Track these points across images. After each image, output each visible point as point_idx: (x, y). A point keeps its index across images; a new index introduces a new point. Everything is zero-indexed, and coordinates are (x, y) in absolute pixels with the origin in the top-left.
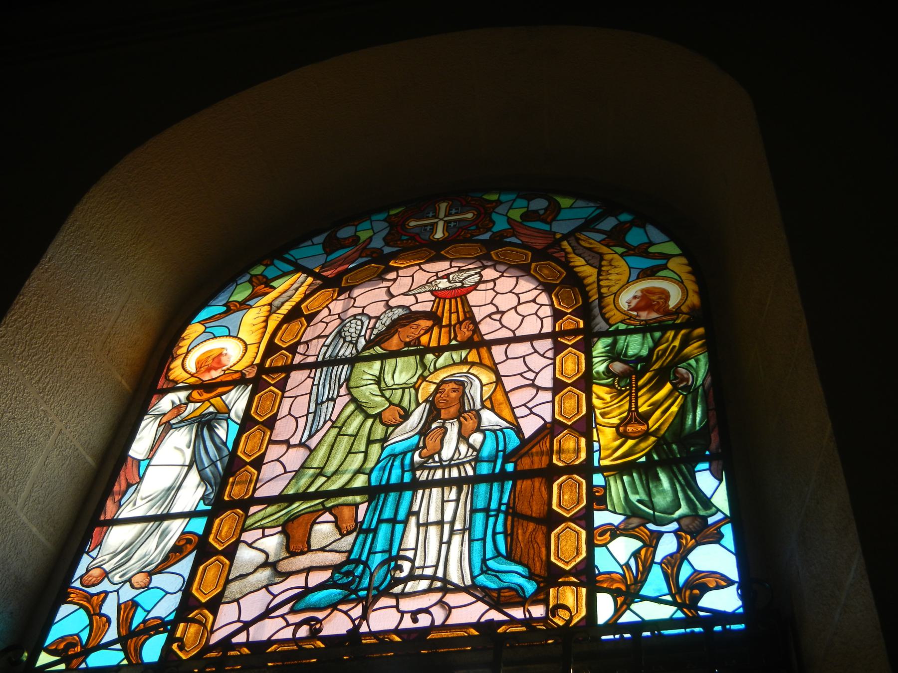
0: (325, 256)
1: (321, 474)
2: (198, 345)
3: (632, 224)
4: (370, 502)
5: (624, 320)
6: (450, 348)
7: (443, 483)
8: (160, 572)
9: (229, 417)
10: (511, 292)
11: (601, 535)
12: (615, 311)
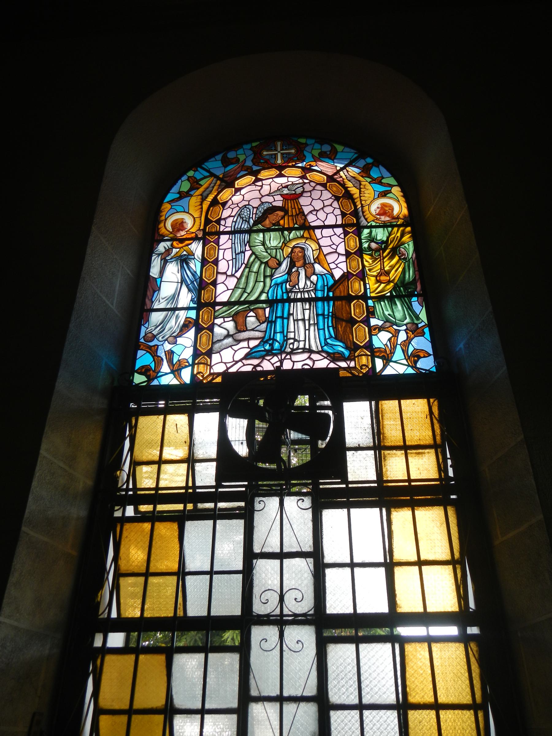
0: (223, 168)
1: (244, 292)
3: (373, 165)
4: (270, 307)
5: (374, 220)
6: (296, 229)
7: (303, 300)
9: (195, 258)
10: (319, 199)
11: (374, 330)
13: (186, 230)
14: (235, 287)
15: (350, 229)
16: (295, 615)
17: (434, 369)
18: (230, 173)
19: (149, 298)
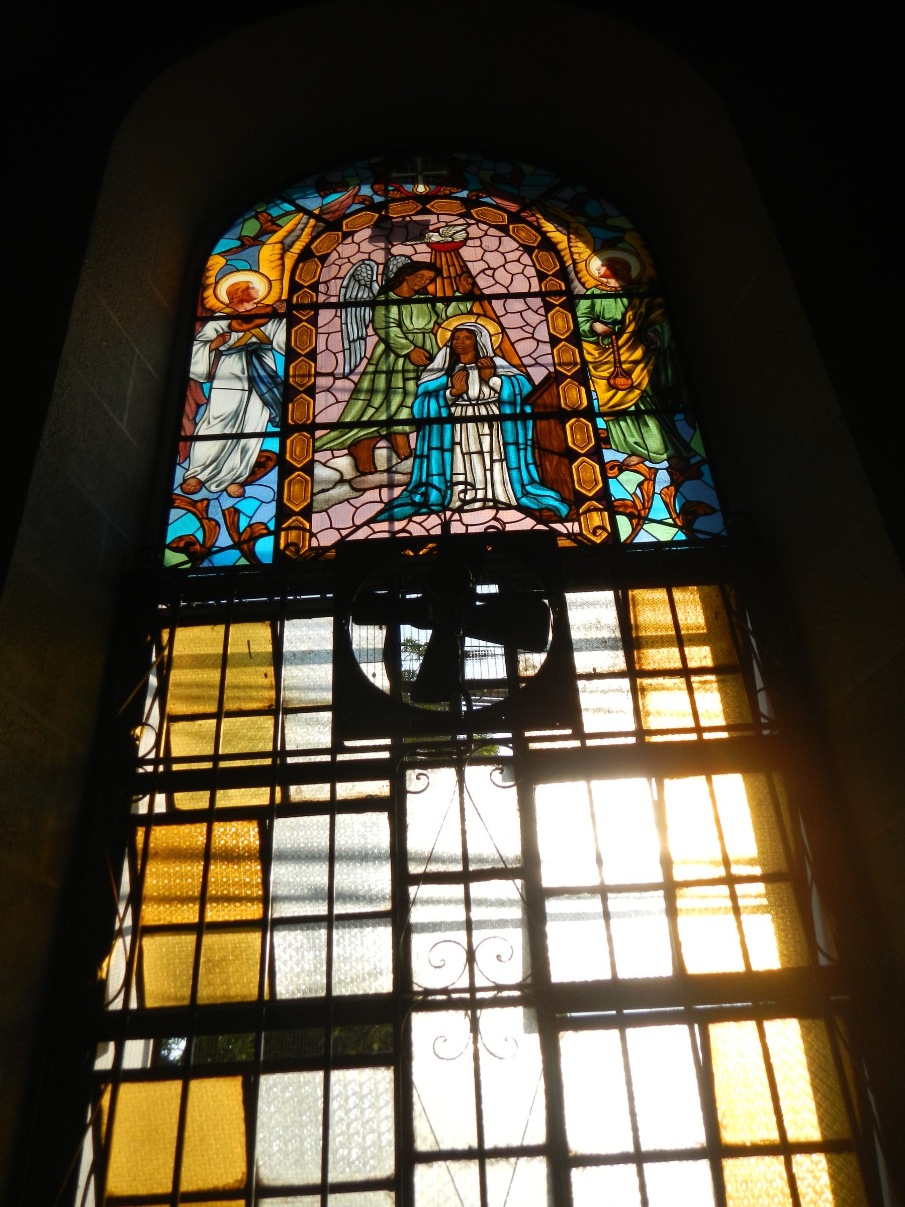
0: (320, 199)
2: (224, 276)
5: (598, 285)
8: (250, 484)
9: (273, 348)
10: (496, 250)
11: (612, 468)
12: (588, 277)
13: (255, 301)
14: (351, 398)
15: (556, 301)
16: (499, 988)
17: (724, 533)
18: (333, 206)
19: (189, 418)
